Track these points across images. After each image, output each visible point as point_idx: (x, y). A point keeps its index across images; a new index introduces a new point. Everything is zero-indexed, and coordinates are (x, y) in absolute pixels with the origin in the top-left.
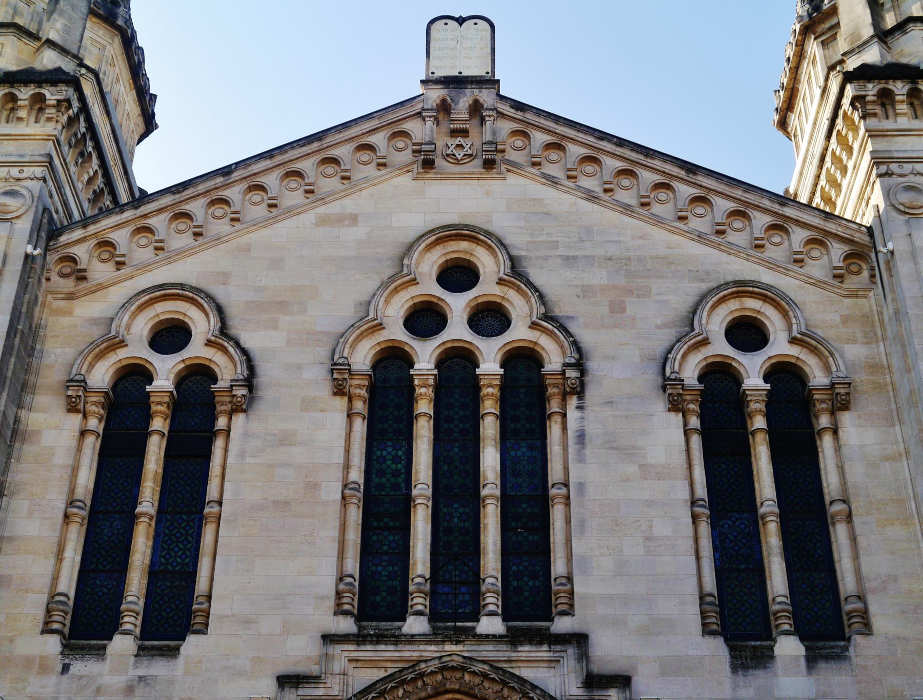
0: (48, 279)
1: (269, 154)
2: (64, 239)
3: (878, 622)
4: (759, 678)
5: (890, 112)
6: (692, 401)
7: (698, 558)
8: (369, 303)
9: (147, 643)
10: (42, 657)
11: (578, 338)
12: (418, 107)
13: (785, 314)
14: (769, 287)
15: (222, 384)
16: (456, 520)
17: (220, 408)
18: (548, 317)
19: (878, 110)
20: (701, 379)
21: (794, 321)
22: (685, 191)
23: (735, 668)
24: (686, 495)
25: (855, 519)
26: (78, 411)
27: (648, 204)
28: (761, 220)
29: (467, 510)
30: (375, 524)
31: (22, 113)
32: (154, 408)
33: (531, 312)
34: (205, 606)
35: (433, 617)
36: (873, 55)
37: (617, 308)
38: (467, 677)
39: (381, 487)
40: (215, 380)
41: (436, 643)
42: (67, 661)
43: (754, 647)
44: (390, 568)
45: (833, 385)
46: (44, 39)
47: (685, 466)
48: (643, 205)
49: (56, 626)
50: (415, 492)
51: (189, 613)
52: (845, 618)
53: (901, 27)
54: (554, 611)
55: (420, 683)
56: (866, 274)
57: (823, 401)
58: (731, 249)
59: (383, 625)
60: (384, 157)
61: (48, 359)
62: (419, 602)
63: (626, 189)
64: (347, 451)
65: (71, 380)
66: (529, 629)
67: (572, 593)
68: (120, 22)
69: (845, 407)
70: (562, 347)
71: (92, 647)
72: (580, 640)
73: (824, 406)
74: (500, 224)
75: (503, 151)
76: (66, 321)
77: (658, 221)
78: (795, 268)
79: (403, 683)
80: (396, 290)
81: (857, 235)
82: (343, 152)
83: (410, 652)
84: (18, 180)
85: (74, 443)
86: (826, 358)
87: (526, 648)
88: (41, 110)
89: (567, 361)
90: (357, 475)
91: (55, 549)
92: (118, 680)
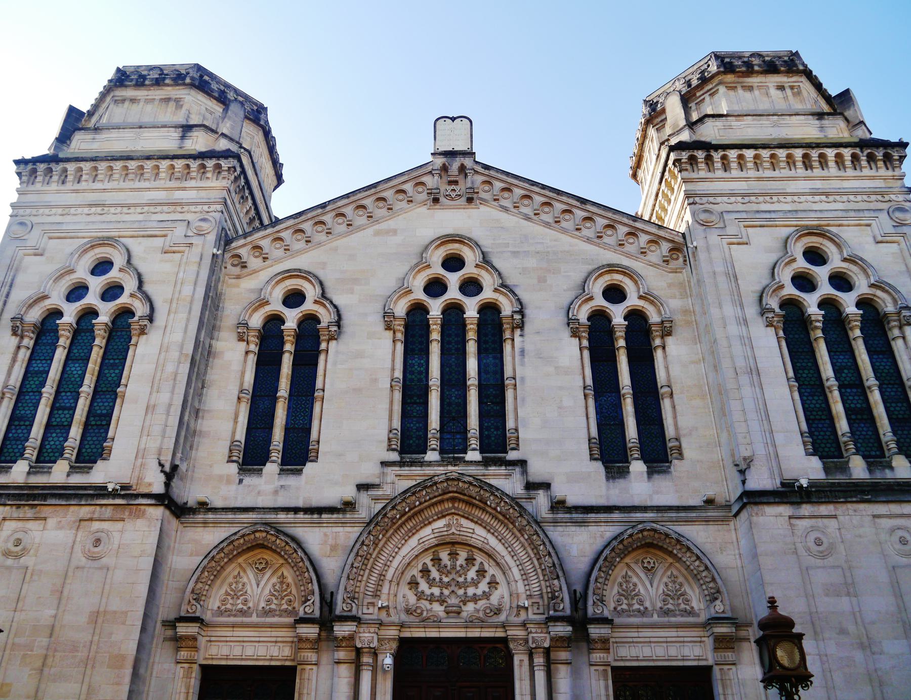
0: (226, 268)
1: (347, 196)
2: (234, 245)
3: (686, 452)
4: (621, 483)
6: (584, 332)
7: (587, 418)
8: (404, 278)
9: (285, 467)
10: (228, 475)
11: (520, 297)
12: (430, 169)
13: (636, 283)
14: (627, 268)
15: (324, 324)
16: (453, 398)
17: (322, 338)
18: (503, 285)
19: (689, 167)
20: (589, 319)
21: (641, 286)
22: (580, 214)
23: (608, 478)
24: (581, 384)
25: (674, 396)
26: (244, 340)
27: (559, 222)
28: (622, 230)
29: (460, 393)
30: (409, 401)
31: (209, 175)
32: (286, 338)
33: (494, 283)
34: (316, 447)
35: (442, 452)
36: (685, 136)
37: (542, 280)
38: (461, 484)
39: (412, 380)
40: (319, 322)
41: (443, 466)
42: (241, 477)
43: (618, 467)
44: (417, 425)
45: (663, 322)
47: (580, 367)
48: (556, 222)
49: (234, 458)
50: (430, 383)
51: (308, 451)
52: (669, 450)
53: (701, 120)
54: (508, 448)
55: (435, 488)
56: (681, 260)
57: (657, 331)
58: (606, 247)
59: (414, 456)
60: (411, 197)
61: (227, 312)
62: (434, 443)
63: (547, 213)
64: (393, 361)
65: (240, 324)
66: (495, 457)
67: (518, 438)
68: (262, 123)
69: (669, 334)
71: (255, 470)
72: (522, 463)
73: (658, 333)
74: (477, 233)
75: (478, 193)
76: (235, 290)
77: (564, 231)
78: (642, 256)
79: (426, 487)
80: (419, 271)
81: (676, 238)
82: (389, 194)
83: (429, 471)
84: (208, 212)
85: (242, 358)
86: (659, 307)
88: (219, 172)
89: (514, 310)
90: (399, 374)
91: (233, 416)
92: (270, 488)
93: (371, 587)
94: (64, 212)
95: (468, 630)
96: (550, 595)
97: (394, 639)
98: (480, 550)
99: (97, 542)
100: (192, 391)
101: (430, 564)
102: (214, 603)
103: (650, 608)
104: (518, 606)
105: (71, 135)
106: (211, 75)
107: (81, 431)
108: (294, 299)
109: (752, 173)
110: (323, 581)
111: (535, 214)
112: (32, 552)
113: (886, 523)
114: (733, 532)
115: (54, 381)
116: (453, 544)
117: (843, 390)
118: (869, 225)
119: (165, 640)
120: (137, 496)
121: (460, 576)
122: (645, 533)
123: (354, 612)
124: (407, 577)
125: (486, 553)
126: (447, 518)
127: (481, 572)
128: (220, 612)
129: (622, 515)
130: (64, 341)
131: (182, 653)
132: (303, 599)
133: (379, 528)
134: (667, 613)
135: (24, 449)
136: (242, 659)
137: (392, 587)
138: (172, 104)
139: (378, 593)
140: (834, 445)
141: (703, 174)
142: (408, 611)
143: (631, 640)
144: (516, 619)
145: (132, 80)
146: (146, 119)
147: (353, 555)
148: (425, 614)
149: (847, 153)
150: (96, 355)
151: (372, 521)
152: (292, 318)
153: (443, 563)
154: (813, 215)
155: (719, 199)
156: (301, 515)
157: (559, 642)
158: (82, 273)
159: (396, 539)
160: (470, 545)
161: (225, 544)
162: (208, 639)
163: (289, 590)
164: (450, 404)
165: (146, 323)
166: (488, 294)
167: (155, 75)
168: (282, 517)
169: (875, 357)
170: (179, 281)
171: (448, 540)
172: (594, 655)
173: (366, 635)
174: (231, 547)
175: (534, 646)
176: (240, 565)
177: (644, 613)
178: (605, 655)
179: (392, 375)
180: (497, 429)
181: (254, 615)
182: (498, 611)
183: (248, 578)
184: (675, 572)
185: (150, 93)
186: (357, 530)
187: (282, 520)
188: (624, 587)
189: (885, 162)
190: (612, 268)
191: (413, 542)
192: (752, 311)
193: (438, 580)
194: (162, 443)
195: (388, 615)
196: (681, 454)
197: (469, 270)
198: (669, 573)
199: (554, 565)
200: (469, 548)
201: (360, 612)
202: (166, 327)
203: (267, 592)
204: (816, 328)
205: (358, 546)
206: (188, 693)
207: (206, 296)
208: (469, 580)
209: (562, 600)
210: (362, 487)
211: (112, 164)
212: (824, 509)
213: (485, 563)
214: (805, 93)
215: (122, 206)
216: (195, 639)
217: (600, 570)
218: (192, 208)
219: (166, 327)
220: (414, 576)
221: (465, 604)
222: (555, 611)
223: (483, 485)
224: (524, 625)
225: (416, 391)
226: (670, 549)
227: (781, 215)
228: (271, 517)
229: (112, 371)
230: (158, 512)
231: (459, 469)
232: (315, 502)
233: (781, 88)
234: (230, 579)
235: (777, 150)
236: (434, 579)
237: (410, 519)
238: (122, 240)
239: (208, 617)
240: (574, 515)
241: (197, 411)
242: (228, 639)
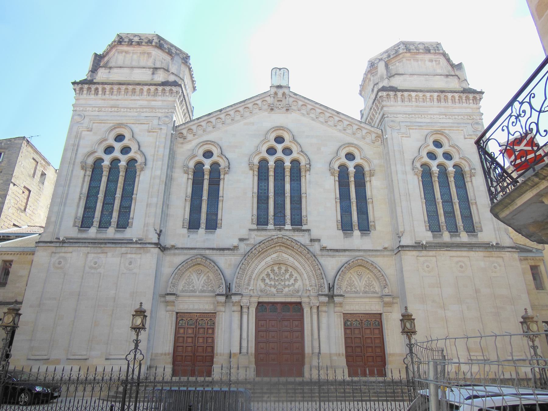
1: (231, 106)
3: (378, 228)
5: (389, 100)
8: (258, 146)
12: (269, 94)
13: (360, 152)
18: (302, 151)
20: (339, 168)
22: (337, 119)
23: (344, 238)
24: (334, 197)
25: (374, 203)
26: (187, 173)
30: (260, 202)
36: (385, 83)
39: (261, 193)
41: (275, 231)
44: (264, 213)
46: (171, 72)
49: (185, 226)
50: (270, 195)
52: (370, 226)
55: (272, 241)
56: (380, 142)
62: (271, 221)
64: (253, 184)
65: (184, 166)
68: (188, 64)
69: (373, 176)
70: (305, 159)
72: (309, 230)
74: (291, 126)
81: (379, 132)
82: (250, 106)
84: (168, 113)
87: (297, 233)
90: (256, 190)
93: (246, 281)
94: (99, 110)
95: (286, 298)
96: (320, 286)
97: (256, 302)
98: (291, 266)
99: (130, 263)
100: (166, 197)
101: (270, 272)
102: (180, 287)
103: (359, 291)
104: (307, 290)
105: (98, 69)
106: (163, 39)
107: (118, 214)
108: (208, 154)
109: (414, 104)
110: (226, 279)
111: (317, 118)
112: (102, 267)
113: (456, 259)
114: (394, 261)
115: (103, 191)
116: (280, 264)
117: (444, 203)
118: (462, 130)
119: (161, 302)
120: (146, 243)
121: (283, 277)
122: (359, 261)
123: (240, 292)
124: (261, 277)
125: (293, 268)
126: (278, 253)
127: (291, 276)
128: (183, 291)
129: (350, 253)
130: (105, 173)
131: (169, 307)
132: (218, 286)
133: (249, 257)
134: (365, 292)
135: (93, 222)
136: (193, 310)
137: (255, 282)
138: (146, 55)
139: (249, 284)
140: (438, 227)
141: (392, 103)
142: (261, 291)
143: (351, 303)
144: (305, 294)
145: (125, 42)
146: (135, 64)
147: (239, 268)
148: (268, 292)
149: (456, 95)
150: (121, 180)
151: (246, 255)
152: (207, 164)
153: (275, 272)
154: (439, 125)
155: (399, 115)
156: (215, 252)
157: (323, 303)
158: (111, 141)
159: (256, 262)
160: (287, 265)
161: (184, 263)
162: (179, 302)
163: (211, 282)
164: (278, 204)
165: (143, 166)
166: (295, 155)
167: (136, 39)
168: (207, 252)
169: (459, 189)
170: (157, 146)
171: (278, 263)
172: (336, 309)
173: (245, 301)
174: (187, 264)
175: (313, 305)
176: (190, 272)
177: (356, 292)
178: (341, 309)
179: (253, 191)
180: (298, 215)
181: (197, 292)
182: (298, 291)
183: (194, 277)
184: (370, 276)
185: (135, 49)
186: (239, 258)
187: (207, 253)
188: (349, 282)
189: (473, 100)
190: (350, 144)
191: (263, 263)
192: (409, 168)
193: (273, 278)
194: (155, 221)
195: (253, 292)
196: (375, 228)
197: (286, 144)
198: (367, 277)
199: (321, 273)
200: (287, 266)
201: (242, 292)
202: (152, 168)
203: (202, 282)
204: (435, 176)
205: (240, 265)
206: (172, 323)
207: (170, 153)
208: (286, 278)
209: (324, 288)
210: (241, 240)
211: (120, 86)
212: (431, 253)
213: (293, 272)
214: (441, 63)
215: (127, 108)
216: (174, 302)
217: (340, 275)
218: (160, 110)
219: (152, 168)
220: (263, 277)
221: (284, 288)
222: (321, 292)
223: (293, 240)
224: (308, 297)
225: (263, 198)
226: (368, 267)
227: (425, 124)
228: (203, 252)
229: (129, 187)
230: (157, 250)
231: (283, 233)
232: (221, 247)
233: (431, 61)
234: (186, 278)
235: (426, 93)
236: (272, 278)
237: (262, 254)
238: (128, 125)
239: (178, 293)
240: (330, 253)
241: (168, 205)
242: (187, 302)
